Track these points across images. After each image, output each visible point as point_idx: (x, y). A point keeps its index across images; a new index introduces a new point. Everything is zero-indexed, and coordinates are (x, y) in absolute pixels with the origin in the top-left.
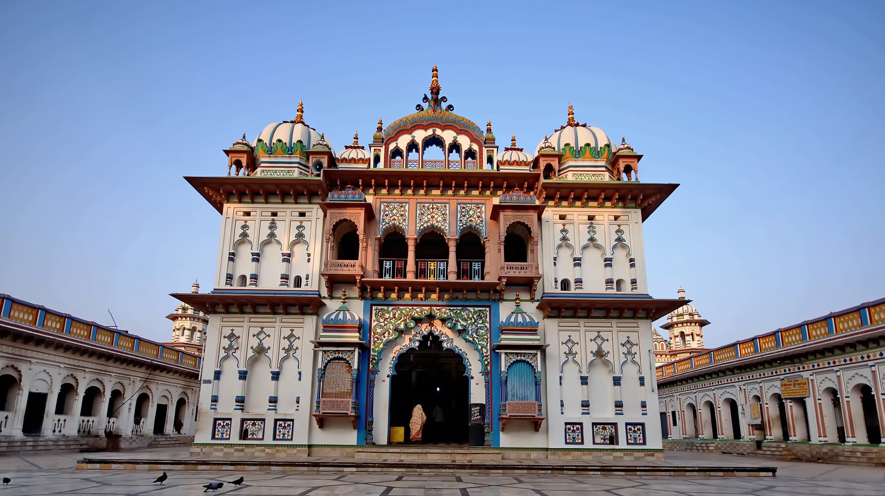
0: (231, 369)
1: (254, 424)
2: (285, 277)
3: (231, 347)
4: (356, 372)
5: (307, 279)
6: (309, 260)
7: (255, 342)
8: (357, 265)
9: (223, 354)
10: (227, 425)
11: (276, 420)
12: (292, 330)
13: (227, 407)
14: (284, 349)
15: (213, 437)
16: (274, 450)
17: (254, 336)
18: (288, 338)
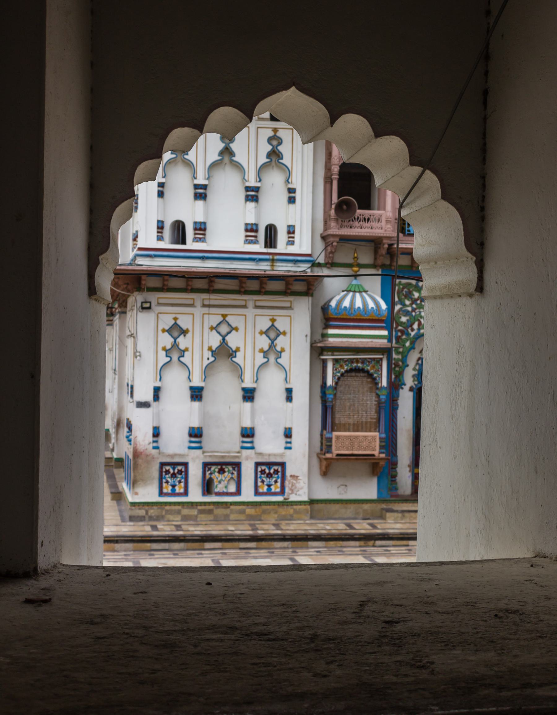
0: (176, 384)
1: (221, 471)
2: (251, 229)
3: (175, 345)
4: (385, 392)
5: (291, 231)
6: (292, 200)
7: (215, 341)
8: (383, 219)
9: (163, 359)
10: (180, 472)
11: (257, 464)
12: (273, 320)
13: (175, 444)
14: (261, 351)
15: (161, 493)
16: (259, 510)
17: (212, 328)
18: (266, 333)
